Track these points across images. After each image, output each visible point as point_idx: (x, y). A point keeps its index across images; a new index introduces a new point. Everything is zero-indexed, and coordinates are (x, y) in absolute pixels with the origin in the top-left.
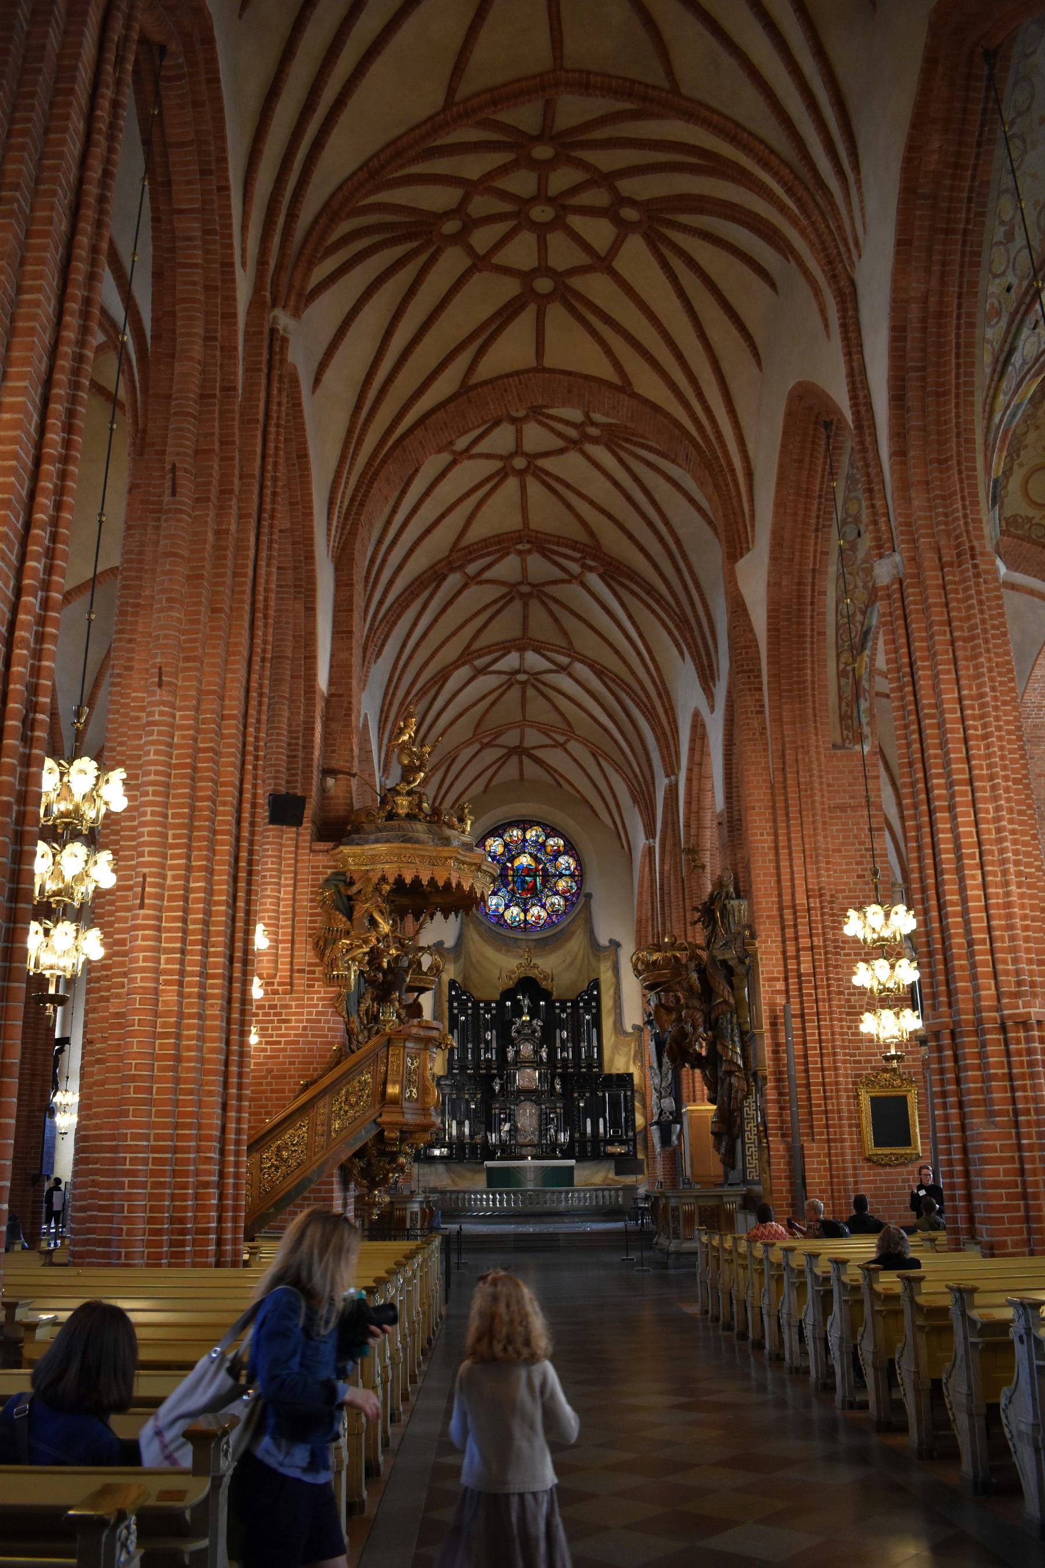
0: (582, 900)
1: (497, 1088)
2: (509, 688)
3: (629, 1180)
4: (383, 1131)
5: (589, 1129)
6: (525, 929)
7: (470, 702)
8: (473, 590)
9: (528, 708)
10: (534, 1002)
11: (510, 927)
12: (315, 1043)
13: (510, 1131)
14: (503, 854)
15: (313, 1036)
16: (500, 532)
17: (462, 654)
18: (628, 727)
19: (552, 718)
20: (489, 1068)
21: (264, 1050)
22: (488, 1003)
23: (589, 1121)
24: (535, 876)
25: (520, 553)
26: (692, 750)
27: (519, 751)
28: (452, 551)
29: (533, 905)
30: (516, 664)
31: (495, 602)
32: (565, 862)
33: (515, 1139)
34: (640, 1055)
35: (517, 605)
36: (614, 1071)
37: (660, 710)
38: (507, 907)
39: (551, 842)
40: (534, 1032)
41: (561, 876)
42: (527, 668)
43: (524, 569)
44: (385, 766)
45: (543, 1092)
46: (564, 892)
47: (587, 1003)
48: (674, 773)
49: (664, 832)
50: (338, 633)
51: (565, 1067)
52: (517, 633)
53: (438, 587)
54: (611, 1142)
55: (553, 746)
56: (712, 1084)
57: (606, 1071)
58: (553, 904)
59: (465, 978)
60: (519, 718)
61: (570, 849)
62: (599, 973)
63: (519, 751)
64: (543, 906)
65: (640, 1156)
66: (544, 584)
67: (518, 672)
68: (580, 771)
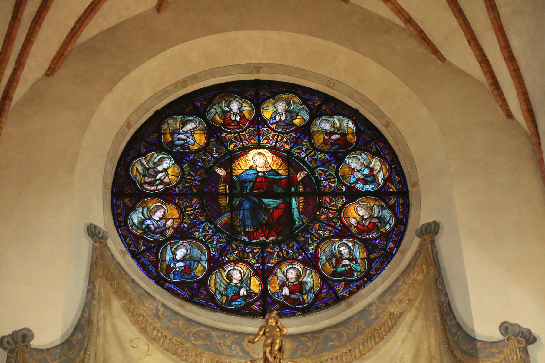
14: (204, 149)
24: (287, 196)
29: (283, 259)
46: (362, 229)
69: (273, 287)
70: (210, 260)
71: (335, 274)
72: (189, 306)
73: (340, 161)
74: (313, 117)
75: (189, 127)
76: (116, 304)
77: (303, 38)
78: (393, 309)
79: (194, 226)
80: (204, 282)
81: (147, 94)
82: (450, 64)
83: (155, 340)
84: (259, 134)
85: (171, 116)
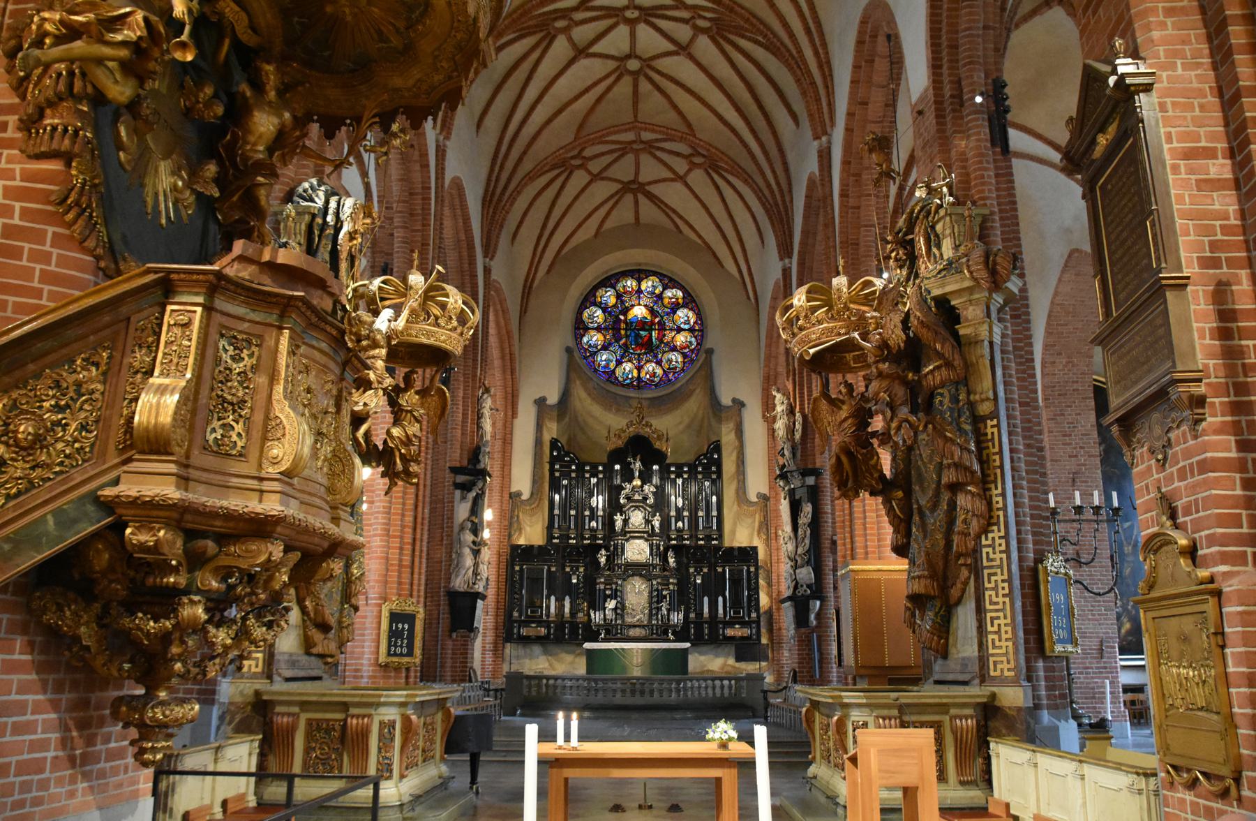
0: (703, 356)
1: (603, 560)
3: (750, 667)
4: (120, 526)
5: (706, 610)
6: (639, 387)
7: (572, 95)
9: (640, 106)
10: (647, 464)
11: (623, 386)
13: (615, 609)
14: (615, 306)
18: (760, 124)
19: (670, 117)
20: (594, 537)
22: (594, 466)
23: (706, 599)
24: (650, 330)
26: (854, 82)
27: (635, 188)
29: (648, 361)
30: (625, 47)
32: (683, 314)
33: (622, 617)
34: (767, 526)
36: (736, 544)
37: (808, 53)
38: (619, 363)
39: (669, 293)
40: (645, 499)
41: (679, 330)
42: (638, 52)
45: (654, 567)
47: (707, 468)
48: (825, 133)
49: (802, 243)
51: (680, 538)
54: (730, 624)
55: (672, 180)
56: (903, 525)
57: (727, 543)
58: (670, 361)
59: (569, 440)
60: (631, 119)
61: (690, 301)
62: (719, 434)
63: (635, 188)
64: (659, 363)
65: (764, 641)
67: (628, 57)
68: (703, 211)
69: (642, 375)
70: (617, 360)
71: (669, 369)
72: (608, 383)
73: (674, 313)
74: (664, 289)
75: (609, 294)
76: (578, 383)
77: (662, 253)
78: (691, 387)
79: (610, 344)
80: (613, 371)
81: (590, 279)
82: (727, 271)
83: (593, 399)
84: (639, 298)
85: (600, 288)
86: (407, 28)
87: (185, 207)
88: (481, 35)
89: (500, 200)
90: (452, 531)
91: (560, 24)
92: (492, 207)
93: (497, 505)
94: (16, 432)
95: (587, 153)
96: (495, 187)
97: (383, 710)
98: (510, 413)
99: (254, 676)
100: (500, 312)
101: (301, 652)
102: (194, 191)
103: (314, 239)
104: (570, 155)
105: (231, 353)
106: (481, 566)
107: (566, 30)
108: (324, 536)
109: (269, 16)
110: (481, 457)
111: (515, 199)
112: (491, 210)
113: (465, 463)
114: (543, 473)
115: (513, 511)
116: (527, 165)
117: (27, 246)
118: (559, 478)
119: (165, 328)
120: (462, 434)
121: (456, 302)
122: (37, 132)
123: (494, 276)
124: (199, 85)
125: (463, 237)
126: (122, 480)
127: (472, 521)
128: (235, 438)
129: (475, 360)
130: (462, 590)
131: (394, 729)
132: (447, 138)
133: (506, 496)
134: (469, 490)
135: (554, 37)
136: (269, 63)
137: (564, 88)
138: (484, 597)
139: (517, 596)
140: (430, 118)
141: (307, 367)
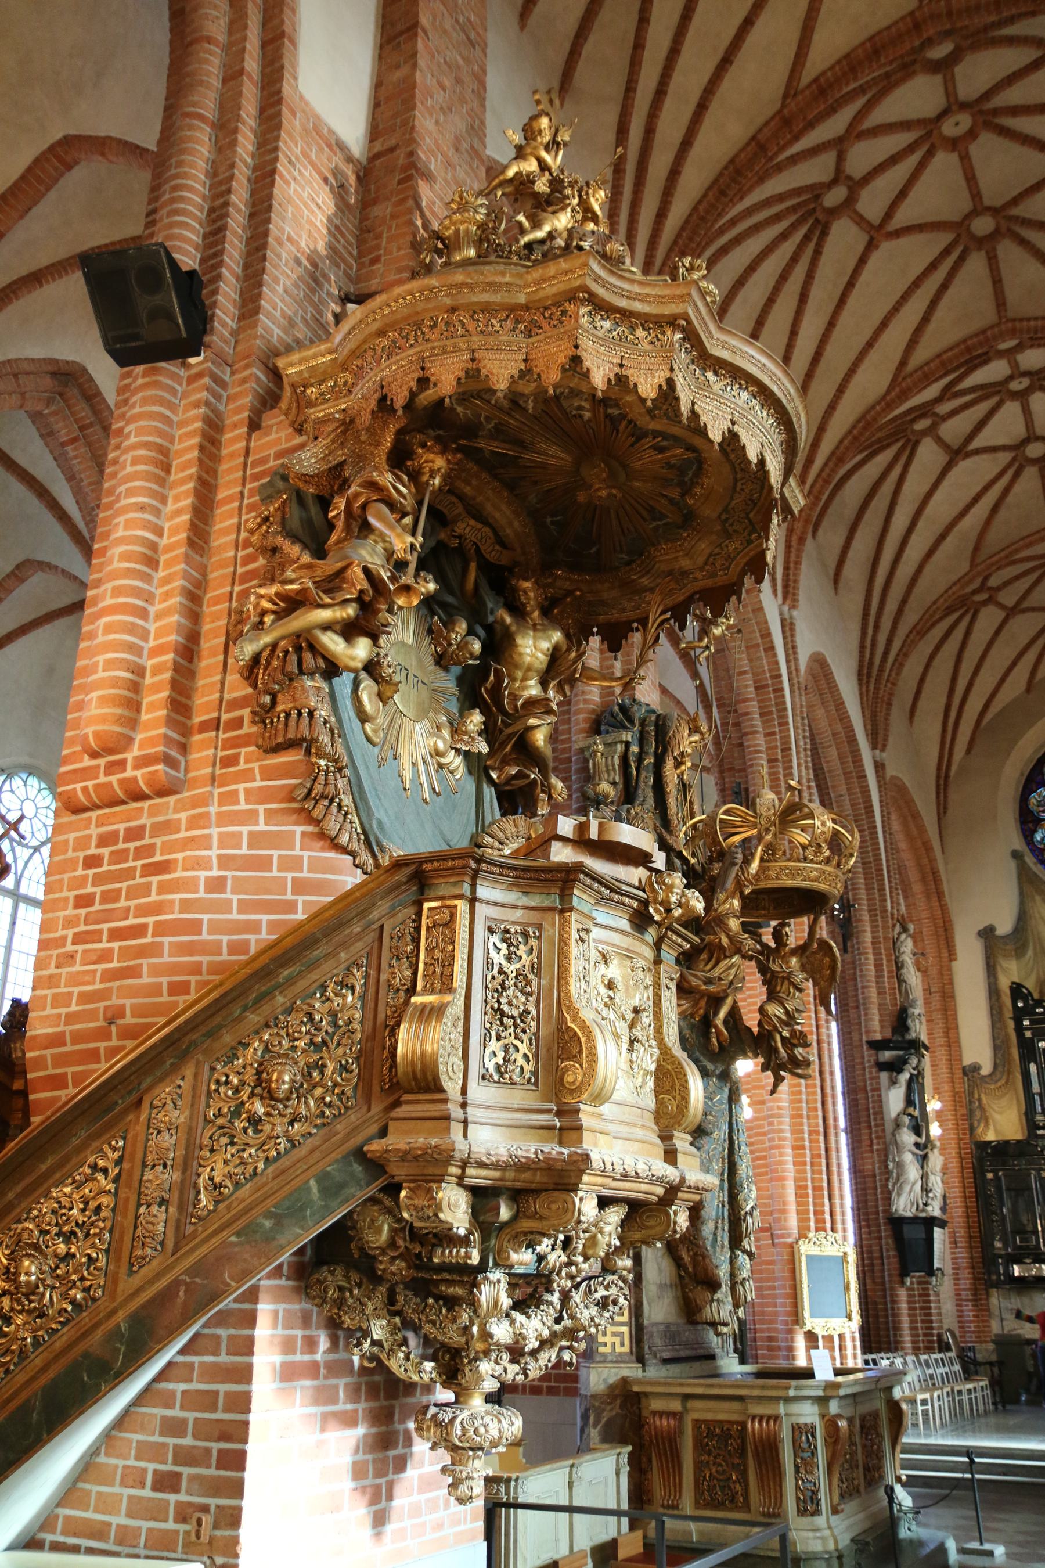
2: (1017, 474)
8: (886, 247)
12: (253, 927)
15: (244, 907)
16: (873, 29)
17: (893, 380)
21: (105, 956)
25: (953, 144)
28: (785, 96)
30: (1019, 430)
31: (933, 266)
35: (976, 264)
43: (971, 178)
44: (786, 587)
50: (389, 41)
52: (984, 314)
53: (817, 253)
66: (1015, 201)
76: (1038, 898)
86: (683, 495)
87: (452, 772)
88: (772, 481)
89: (881, 670)
90: (883, 1131)
91: (921, 425)
92: (873, 680)
93: (946, 1087)
94: (270, 1080)
95: (993, 582)
96: (872, 654)
97: (796, 1408)
98: (945, 954)
99: (620, 1359)
100: (909, 818)
101: (682, 1321)
102: (457, 751)
103: (631, 773)
104: (969, 589)
105: (504, 951)
106: (932, 1178)
107: (931, 431)
108: (659, 1180)
109: (516, 524)
110: (909, 1021)
111: (902, 665)
112: (872, 686)
113: (888, 1034)
114: (1007, 1035)
115: (971, 1094)
116: (911, 617)
117: (276, 853)
118: (1032, 1039)
119: (423, 933)
120: (879, 993)
121: (823, 824)
122: (272, 722)
123: (890, 772)
124: (449, 624)
125: (839, 728)
126: (391, 1129)
127: (909, 1115)
128: (521, 1061)
129: (882, 889)
130: (909, 1214)
131: (814, 1436)
132: (793, 607)
133: (959, 1074)
134: (900, 1071)
135: (917, 443)
136: (526, 579)
137: (942, 507)
138: (943, 1224)
139: (995, 1218)
140: (734, 599)
141: (604, 956)
